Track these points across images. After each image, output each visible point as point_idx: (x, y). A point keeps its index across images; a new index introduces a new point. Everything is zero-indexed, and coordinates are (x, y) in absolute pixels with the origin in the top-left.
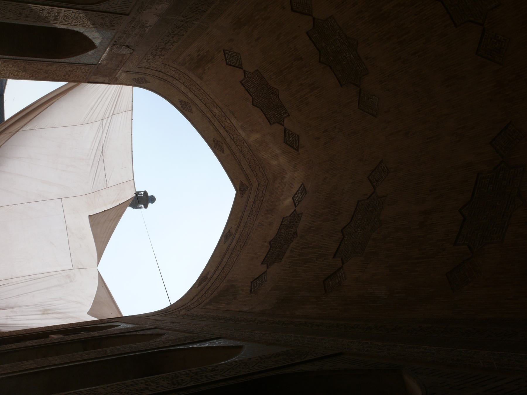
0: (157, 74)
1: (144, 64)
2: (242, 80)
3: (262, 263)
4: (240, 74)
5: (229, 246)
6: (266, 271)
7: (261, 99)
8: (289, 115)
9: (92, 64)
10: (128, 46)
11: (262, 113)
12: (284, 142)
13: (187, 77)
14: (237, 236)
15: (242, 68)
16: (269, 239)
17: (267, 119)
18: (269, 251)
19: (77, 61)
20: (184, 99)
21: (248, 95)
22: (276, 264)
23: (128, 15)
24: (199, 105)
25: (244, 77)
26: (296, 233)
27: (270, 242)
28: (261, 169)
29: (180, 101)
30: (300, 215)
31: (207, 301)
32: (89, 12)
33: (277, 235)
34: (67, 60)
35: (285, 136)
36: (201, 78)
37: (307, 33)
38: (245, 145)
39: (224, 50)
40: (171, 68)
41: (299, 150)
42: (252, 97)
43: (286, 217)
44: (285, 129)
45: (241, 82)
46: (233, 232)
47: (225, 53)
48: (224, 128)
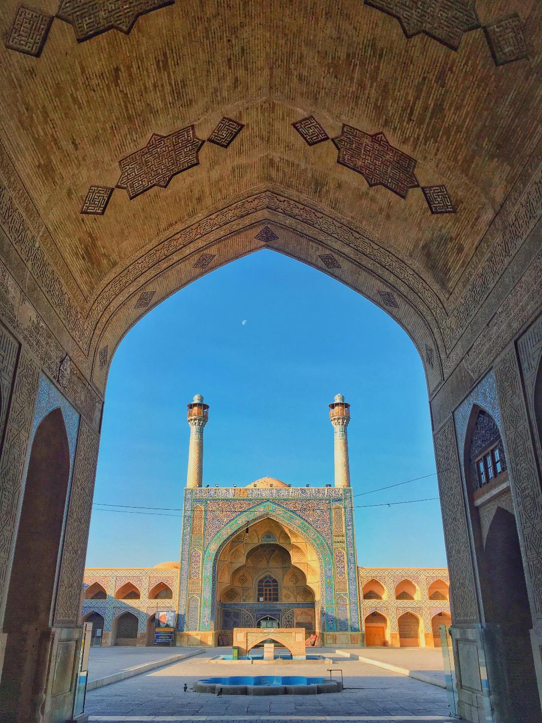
0: (98, 332)
3: (404, 197)
5: (347, 257)
6: (423, 189)
8: (193, 127)
10: (62, 362)
12: (226, 147)
13: (109, 287)
15: (113, 190)
17: (189, 167)
18: (386, 186)
19: (74, 441)
20: (134, 301)
22: (416, 171)
23: (20, 345)
24: (148, 278)
26: (374, 137)
27: (371, 186)
28: (250, 199)
29: (137, 306)
31: (436, 287)
32: (12, 406)
34: (72, 456)
35: (218, 144)
36: (115, 264)
37: (80, 41)
38: (213, 217)
39: (82, 213)
40: (94, 308)
41: (243, 123)
43: (339, 157)
44: (210, 140)
45: (131, 198)
46: (328, 252)
47: (86, 213)
48: (185, 246)
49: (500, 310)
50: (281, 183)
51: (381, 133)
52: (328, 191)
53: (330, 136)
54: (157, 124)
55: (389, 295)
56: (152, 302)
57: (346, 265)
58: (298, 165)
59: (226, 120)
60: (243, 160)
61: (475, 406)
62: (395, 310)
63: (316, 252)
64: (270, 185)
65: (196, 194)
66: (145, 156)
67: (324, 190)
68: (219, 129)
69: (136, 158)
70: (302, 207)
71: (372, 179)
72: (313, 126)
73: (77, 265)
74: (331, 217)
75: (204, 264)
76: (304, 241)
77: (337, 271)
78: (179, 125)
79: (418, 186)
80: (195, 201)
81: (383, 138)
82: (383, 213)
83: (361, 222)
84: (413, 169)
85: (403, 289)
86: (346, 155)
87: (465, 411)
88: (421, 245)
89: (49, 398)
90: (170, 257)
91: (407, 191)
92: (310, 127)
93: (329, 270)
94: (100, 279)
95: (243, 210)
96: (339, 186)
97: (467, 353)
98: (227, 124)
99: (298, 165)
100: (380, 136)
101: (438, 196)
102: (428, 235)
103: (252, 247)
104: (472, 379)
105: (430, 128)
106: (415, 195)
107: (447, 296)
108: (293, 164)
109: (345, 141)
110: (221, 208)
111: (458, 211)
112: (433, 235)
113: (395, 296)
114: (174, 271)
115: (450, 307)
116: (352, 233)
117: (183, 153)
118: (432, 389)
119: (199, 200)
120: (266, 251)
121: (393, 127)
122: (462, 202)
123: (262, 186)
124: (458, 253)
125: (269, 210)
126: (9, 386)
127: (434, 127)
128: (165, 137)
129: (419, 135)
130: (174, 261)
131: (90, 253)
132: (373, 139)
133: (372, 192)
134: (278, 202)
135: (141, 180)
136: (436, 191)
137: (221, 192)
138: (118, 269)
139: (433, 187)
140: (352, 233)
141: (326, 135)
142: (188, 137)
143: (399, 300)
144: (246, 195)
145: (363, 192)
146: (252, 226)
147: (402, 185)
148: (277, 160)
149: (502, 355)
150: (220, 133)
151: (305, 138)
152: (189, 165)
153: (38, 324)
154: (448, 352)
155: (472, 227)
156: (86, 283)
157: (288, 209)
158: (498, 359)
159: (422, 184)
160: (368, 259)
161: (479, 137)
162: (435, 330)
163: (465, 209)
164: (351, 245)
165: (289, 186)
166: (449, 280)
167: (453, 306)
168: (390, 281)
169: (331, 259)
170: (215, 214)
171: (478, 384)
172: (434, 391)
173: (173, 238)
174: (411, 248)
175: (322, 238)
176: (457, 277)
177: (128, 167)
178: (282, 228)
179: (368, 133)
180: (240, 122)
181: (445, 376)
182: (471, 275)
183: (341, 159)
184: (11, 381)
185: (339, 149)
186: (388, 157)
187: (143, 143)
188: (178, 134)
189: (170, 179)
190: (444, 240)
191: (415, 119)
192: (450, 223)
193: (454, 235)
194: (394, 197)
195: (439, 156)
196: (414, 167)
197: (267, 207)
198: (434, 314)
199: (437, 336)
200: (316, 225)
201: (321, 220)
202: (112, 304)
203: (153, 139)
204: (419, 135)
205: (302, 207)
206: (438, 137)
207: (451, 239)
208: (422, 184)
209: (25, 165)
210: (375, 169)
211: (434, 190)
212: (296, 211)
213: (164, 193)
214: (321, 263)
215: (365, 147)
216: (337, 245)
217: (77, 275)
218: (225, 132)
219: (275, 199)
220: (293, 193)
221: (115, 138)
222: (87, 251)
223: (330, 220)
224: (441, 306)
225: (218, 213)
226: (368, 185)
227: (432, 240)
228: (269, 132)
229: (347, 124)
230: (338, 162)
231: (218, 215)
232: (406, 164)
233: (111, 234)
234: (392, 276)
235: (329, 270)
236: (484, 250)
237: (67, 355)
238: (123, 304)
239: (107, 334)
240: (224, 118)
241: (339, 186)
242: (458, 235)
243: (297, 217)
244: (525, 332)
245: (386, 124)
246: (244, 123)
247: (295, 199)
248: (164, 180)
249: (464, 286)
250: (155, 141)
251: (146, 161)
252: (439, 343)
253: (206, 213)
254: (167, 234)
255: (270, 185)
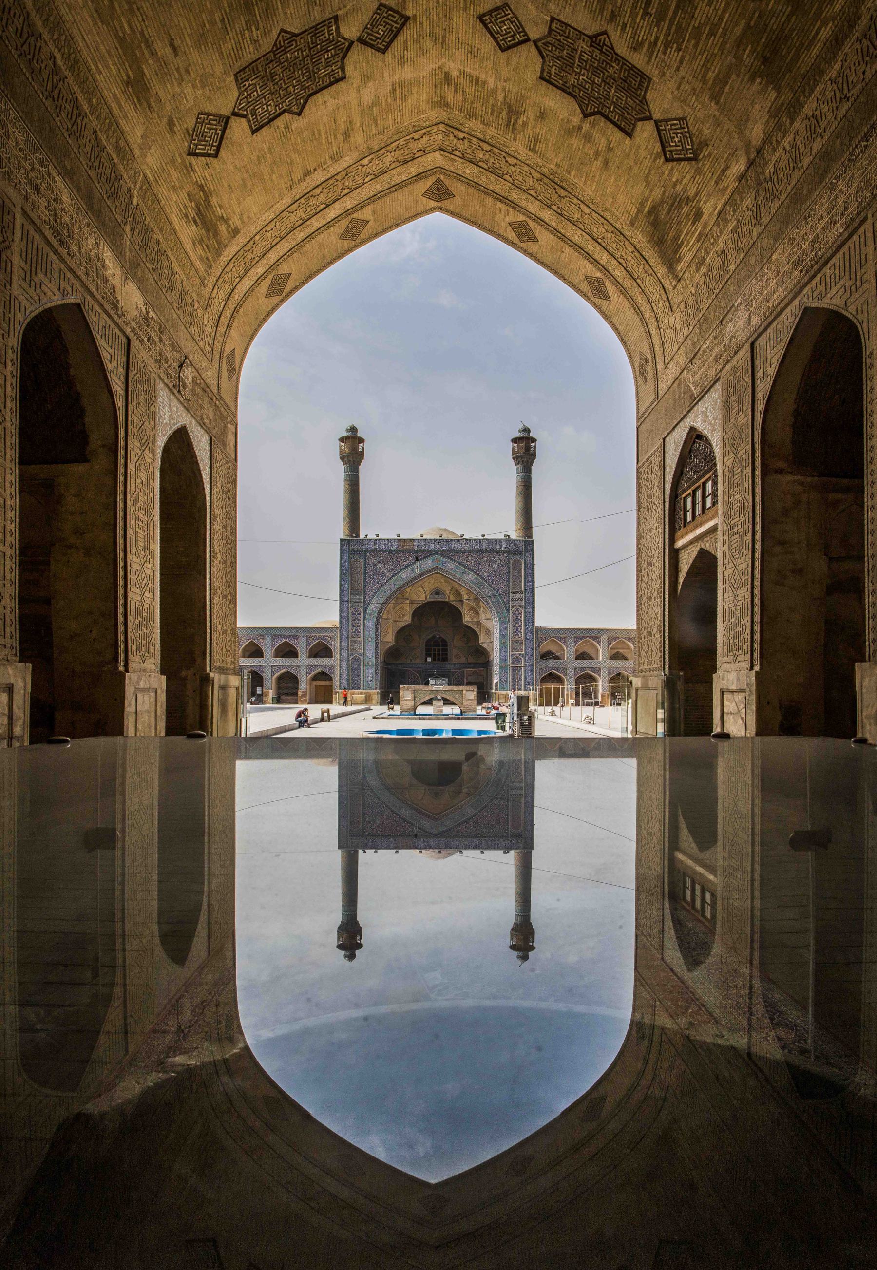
0: (222, 329)
1: (208, 348)
2: (251, 127)
3: (629, 135)
4: (239, 128)
6: (656, 122)
7: (291, 89)
8: (336, 18)
9: (211, 444)
10: (181, 366)
11: (319, 95)
12: (384, 52)
13: (231, 265)
14: (534, 208)
16: (576, 119)
17: (331, 84)
18: (606, 117)
20: (265, 285)
21: (280, 122)
23: (129, 340)
24: (281, 254)
25: (243, 120)
26: (594, 40)
27: (586, 116)
28: (416, 136)
29: (269, 295)
30: (554, 26)
31: (661, 271)
33: (574, 97)
35: (372, 46)
36: (236, 232)
38: (365, 162)
39: (190, 154)
40: (213, 296)
42: (284, 111)
43: (543, 70)
44: (361, 41)
45: (254, 132)
46: (521, 218)
48: (328, 206)
49: (739, 301)
50: (461, 110)
51: (605, 33)
52: (525, 124)
53: (531, 37)
54: (286, 14)
55: (599, 282)
56: (288, 289)
57: (545, 238)
58: (484, 83)
59: (383, 9)
60: (407, 73)
61: (692, 429)
62: (605, 303)
63: (506, 217)
64: (444, 113)
65: (342, 127)
66: (271, 65)
67: (520, 122)
68: (374, 23)
69: (257, 69)
70: (489, 148)
71: (587, 105)
72: (508, 19)
73: (187, 233)
74: (528, 165)
75: (353, 235)
76: (489, 201)
77: (533, 247)
78: (317, 16)
79: (650, 118)
80: (340, 138)
81: (607, 40)
82: (600, 158)
83: (569, 173)
84: (646, 92)
85: (619, 273)
86: (552, 67)
87: (680, 435)
88: (646, 209)
89: (170, 414)
90: (308, 223)
91: (635, 125)
92: (503, 22)
93: (522, 245)
94: (218, 253)
95: (407, 152)
96: (542, 115)
97: (691, 361)
98: (385, 14)
99: (484, 83)
100: (602, 37)
101: (676, 134)
102: (657, 194)
103: (420, 209)
104: (693, 395)
105: (674, 27)
106: (645, 132)
107: (674, 283)
108: (477, 80)
109: (553, 46)
110: (376, 148)
111: (701, 157)
112: (664, 192)
113: (607, 283)
114: (314, 243)
115: (676, 300)
116: (555, 189)
117: (323, 60)
118: (642, 410)
119: (347, 135)
120: (437, 215)
121: (621, 23)
122: (707, 145)
123: (434, 115)
124: (694, 223)
125: (442, 152)
126: (123, 393)
127: (679, 26)
128: (297, 35)
129: (657, 38)
130: (314, 229)
131: (205, 216)
132: (592, 42)
133: (586, 126)
134: (455, 141)
135: (266, 104)
136: (674, 127)
137: (376, 125)
138: (241, 240)
139: (670, 120)
140: (555, 189)
141: (526, 35)
142: (329, 35)
143: (611, 289)
144: (411, 129)
145: (574, 127)
146: (419, 177)
147: (629, 117)
148: (455, 73)
149: (734, 362)
150: (375, 30)
151: (495, 39)
152: (332, 80)
153: (148, 313)
154: (667, 361)
155: (717, 183)
156: (201, 259)
157: (469, 151)
158: (729, 366)
159: (657, 116)
160: (574, 228)
161: (739, 43)
162: (654, 332)
163: (710, 154)
164: (553, 207)
165: (471, 115)
166: (679, 260)
167: (681, 298)
168: (602, 262)
169: (526, 228)
170: (369, 158)
171: (699, 400)
172: (644, 413)
173: (311, 193)
174: (634, 211)
175: (514, 196)
176: (688, 258)
177: (247, 83)
178: (460, 180)
179: (586, 32)
180: (403, 13)
181: (660, 392)
182: (708, 254)
183: (545, 74)
184: (123, 387)
185: (543, 57)
186: (611, 71)
187: (267, 45)
188: (314, 30)
189: (306, 102)
190: (678, 202)
191: (654, 11)
192: (688, 177)
193: (691, 194)
194: (618, 135)
195: (682, 72)
196: (647, 88)
197: (441, 149)
198: (655, 309)
199: (656, 339)
200: (507, 177)
201: (513, 169)
202: (236, 291)
203: (280, 38)
204: (657, 38)
205: (489, 148)
206: (683, 41)
207: (688, 200)
208: (657, 116)
209: (109, 80)
210: (592, 89)
211: (672, 125)
212: (480, 155)
213: (298, 123)
214: (511, 235)
215: (581, 55)
216: (534, 208)
217: (189, 246)
218: (382, 28)
219: (451, 135)
220: (474, 125)
221: (227, 37)
222: (199, 213)
223: (526, 168)
224: (664, 298)
225: (372, 156)
226: (581, 116)
227: (662, 202)
228: (445, 30)
229: (556, 16)
230: (542, 78)
231: (372, 159)
232: (636, 82)
233: (229, 186)
234: (606, 254)
235: (522, 245)
236: (729, 217)
237: (186, 357)
238: (251, 290)
239: (233, 333)
240: (381, 5)
241: (542, 115)
242: (697, 193)
243: (480, 164)
244: (765, 329)
245: (613, 17)
246: (409, 13)
247: (479, 135)
248: (296, 104)
249: (698, 269)
250: (284, 41)
251: (271, 74)
252: (657, 348)
253: (356, 156)
254: (304, 187)
255: (443, 114)
